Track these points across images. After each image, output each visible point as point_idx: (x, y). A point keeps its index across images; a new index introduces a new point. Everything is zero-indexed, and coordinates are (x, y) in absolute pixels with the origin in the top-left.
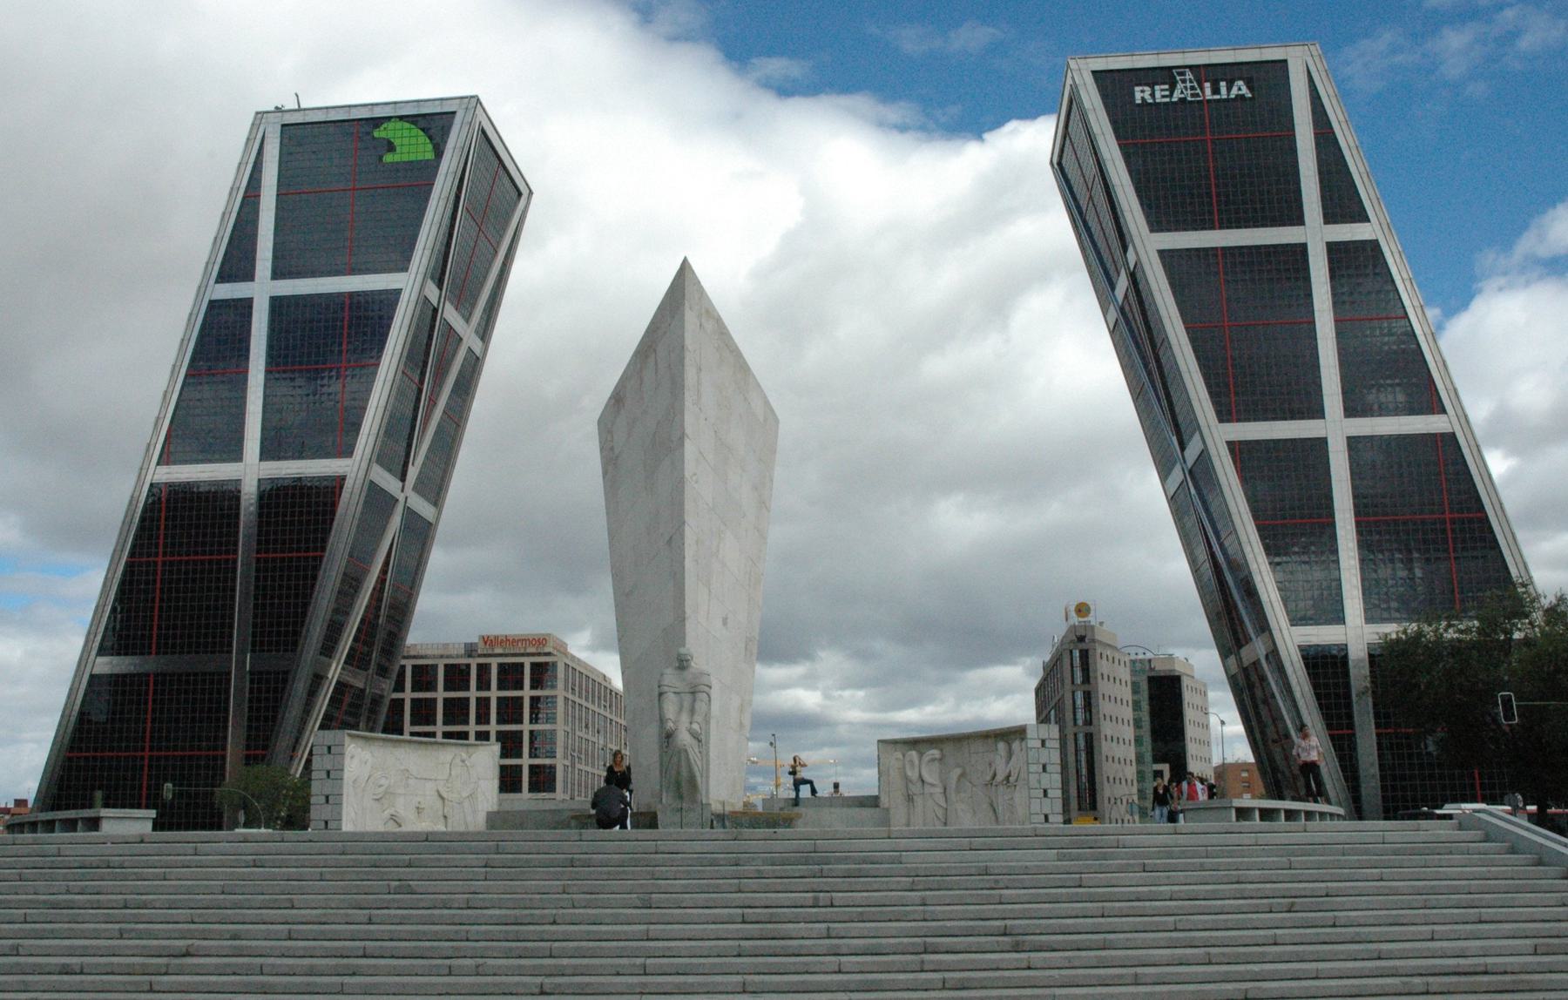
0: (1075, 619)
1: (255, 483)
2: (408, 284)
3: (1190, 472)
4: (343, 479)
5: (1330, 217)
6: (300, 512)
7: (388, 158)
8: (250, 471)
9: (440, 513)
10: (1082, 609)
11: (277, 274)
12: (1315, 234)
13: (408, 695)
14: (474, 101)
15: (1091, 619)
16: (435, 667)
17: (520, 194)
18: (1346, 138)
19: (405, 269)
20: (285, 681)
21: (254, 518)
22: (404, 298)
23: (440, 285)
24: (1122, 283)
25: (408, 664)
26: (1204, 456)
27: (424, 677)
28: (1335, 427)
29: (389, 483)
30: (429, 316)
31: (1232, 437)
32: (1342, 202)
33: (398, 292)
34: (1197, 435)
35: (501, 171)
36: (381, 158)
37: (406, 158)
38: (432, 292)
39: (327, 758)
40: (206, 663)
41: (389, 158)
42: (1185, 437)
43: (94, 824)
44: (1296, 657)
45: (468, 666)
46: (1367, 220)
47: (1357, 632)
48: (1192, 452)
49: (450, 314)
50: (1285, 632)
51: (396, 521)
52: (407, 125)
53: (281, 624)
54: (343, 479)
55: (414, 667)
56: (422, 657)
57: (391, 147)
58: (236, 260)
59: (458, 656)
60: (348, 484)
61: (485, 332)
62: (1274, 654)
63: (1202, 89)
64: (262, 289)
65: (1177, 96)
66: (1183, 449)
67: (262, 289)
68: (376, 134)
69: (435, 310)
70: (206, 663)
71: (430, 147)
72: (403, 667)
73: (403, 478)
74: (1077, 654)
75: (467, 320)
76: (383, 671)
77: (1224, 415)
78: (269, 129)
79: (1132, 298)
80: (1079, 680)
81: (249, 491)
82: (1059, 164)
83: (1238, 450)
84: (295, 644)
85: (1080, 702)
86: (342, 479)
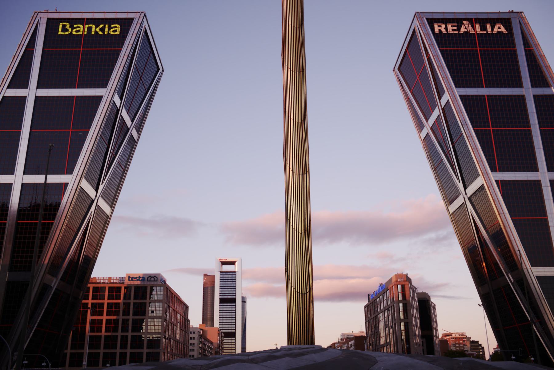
2: (107, 95)
3: (469, 199)
4: (66, 184)
5: (534, 85)
9: (113, 212)
11: (40, 85)
12: (528, 91)
13: (90, 301)
14: (143, 14)
16: (104, 288)
17: (159, 69)
22: (104, 100)
23: (121, 99)
25: (91, 286)
29: (91, 192)
30: (114, 112)
31: (497, 179)
35: (151, 55)
42: (467, 184)
44: (535, 282)
45: (120, 288)
48: (471, 190)
51: (93, 209)
55: (93, 287)
56: (98, 283)
58: (20, 79)
59: (116, 283)
62: (522, 281)
63: (474, 29)
64: (31, 92)
65: (462, 30)
66: (465, 188)
67: (31, 92)
73: (97, 190)
74: (399, 286)
75: (132, 121)
77: (493, 170)
83: (501, 184)
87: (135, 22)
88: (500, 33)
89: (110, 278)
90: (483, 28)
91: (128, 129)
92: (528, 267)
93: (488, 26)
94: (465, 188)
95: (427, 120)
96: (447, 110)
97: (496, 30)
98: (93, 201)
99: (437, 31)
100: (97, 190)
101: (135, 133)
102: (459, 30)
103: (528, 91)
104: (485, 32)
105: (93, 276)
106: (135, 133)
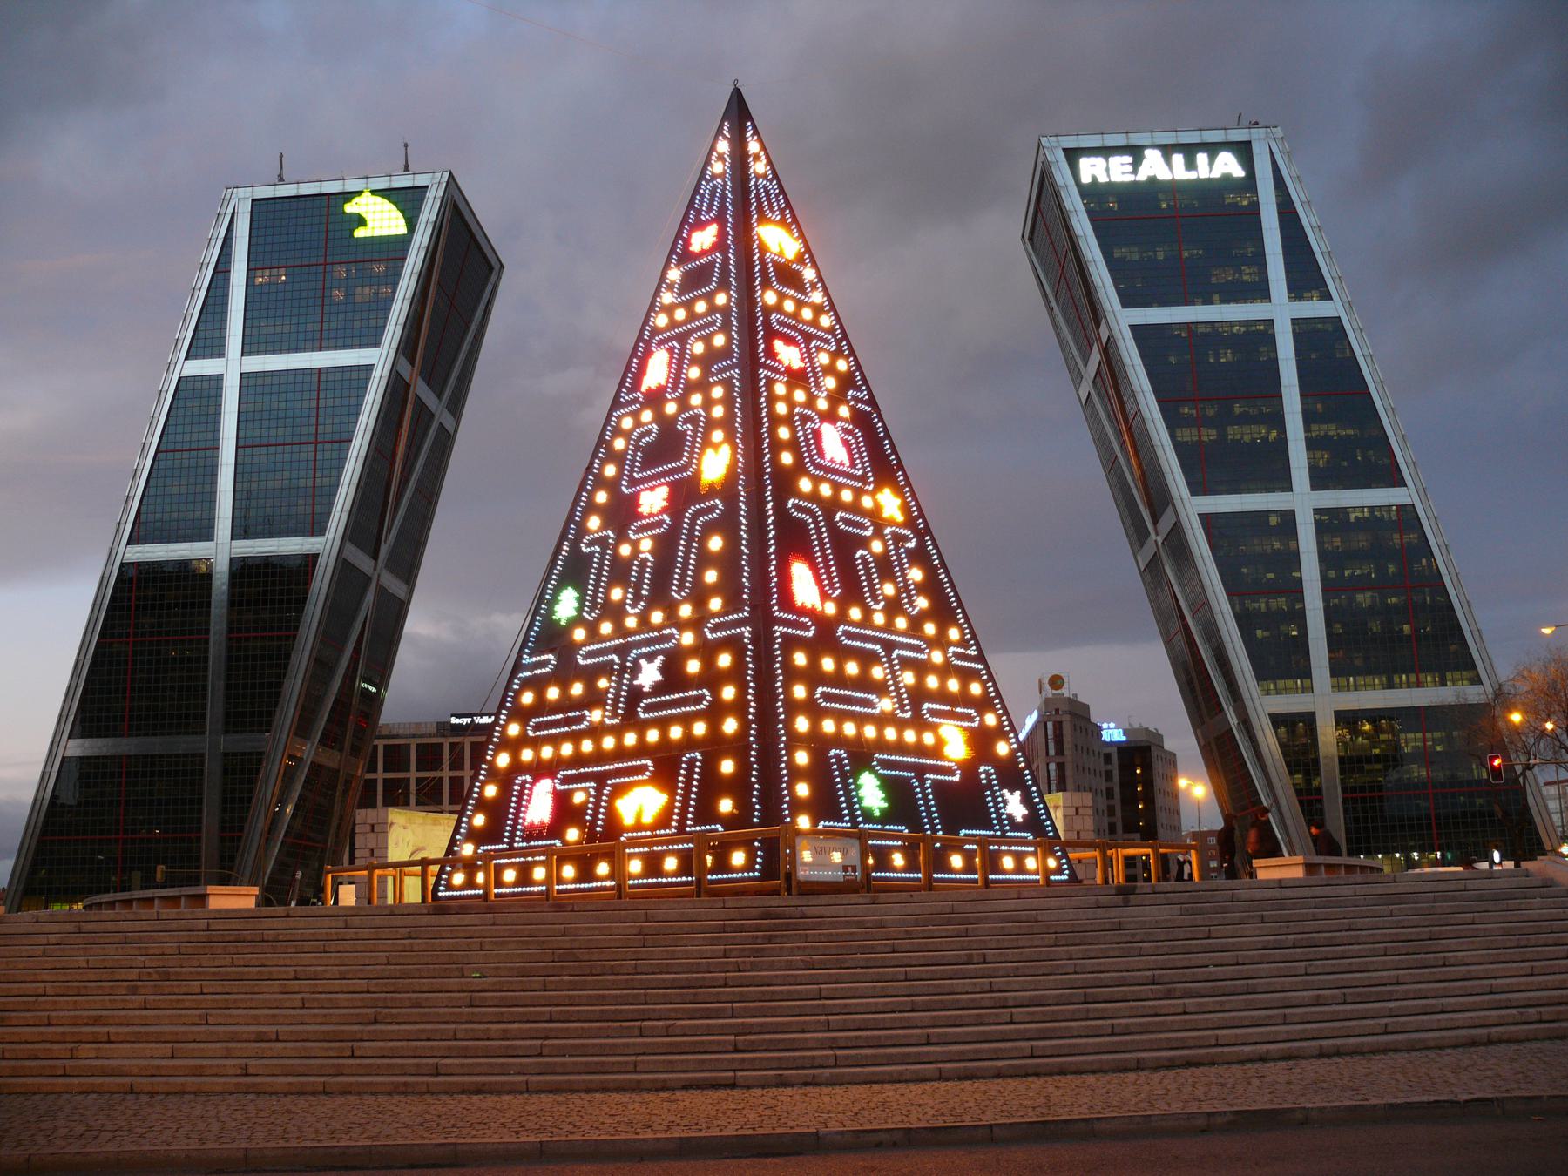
0: (1049, 692)
1: (227, 561)
6: (269, 587)
7: (360, 233)
8: (220, 550)
10: (1056, 682)
12: (1281, 310)
13: (380, 775)
14: (446, 175)
15: (1066, 692)
17: (491, 269)
18: (1307, 219)
19: (377, 344)
20: (260, 762)
21: (225, 597)
22: (376, 373)
23: (413, 365)
24: (1096, 356)
25: (380, 743)
26: (1177, 531)
27: (396, 757)
28: (1303, 500)
29: (363, 562)
32: (1306, 279)
33: (369, 368)
34: (1170, 509)
36: (352, 231)
37: (377, 233)
38: (405, 370)
39: (371, 836)
40: (181, 744)
41: (360, 233)
43: (202, 899)
46: (1330, 298)
47: (1324, 698)
49: (422, 390)
50: (1257, 702)
51: (370, 597)
52: (378, 199)
53: (253, 703)
54: (316, 556)
57: (361, 221)
60: (321, 563)
61: (456, 406)
64: (232, 365)
67: (232, 365)
68: (349, 208)
69: (408, 386)
70: (181, 744)
71: (402, 221)
72: (376, 747)
73: (375, 557)
74: (1050, 725)
75: (439, 396)
76: (355, 751)
78: (240, 210)
79: (1105, 373)
80: (1052, 752)
81: (222, 568)
82: (1030, 239)
84: (269, 724)
85: (1053, 774)
86: (311, 560)
87: (430, 194)
88: (1227, 178)
89: (418, 725)
90: (1191, 164)
91: (433, 415)
92: (1255, 695)
93: (1202, 158)
94: (1155, 522)
95: (1086, 364)
96: (1110, 353)
97: (1217, 173)
98: (370, 579)
99: (1086, 179)
100: (375, 557)
101: (447, 420)
102: (1135, 172)
103: (1281, 310)
104: (1192, 175)
105: (381, 722)
106: (447, 420)
